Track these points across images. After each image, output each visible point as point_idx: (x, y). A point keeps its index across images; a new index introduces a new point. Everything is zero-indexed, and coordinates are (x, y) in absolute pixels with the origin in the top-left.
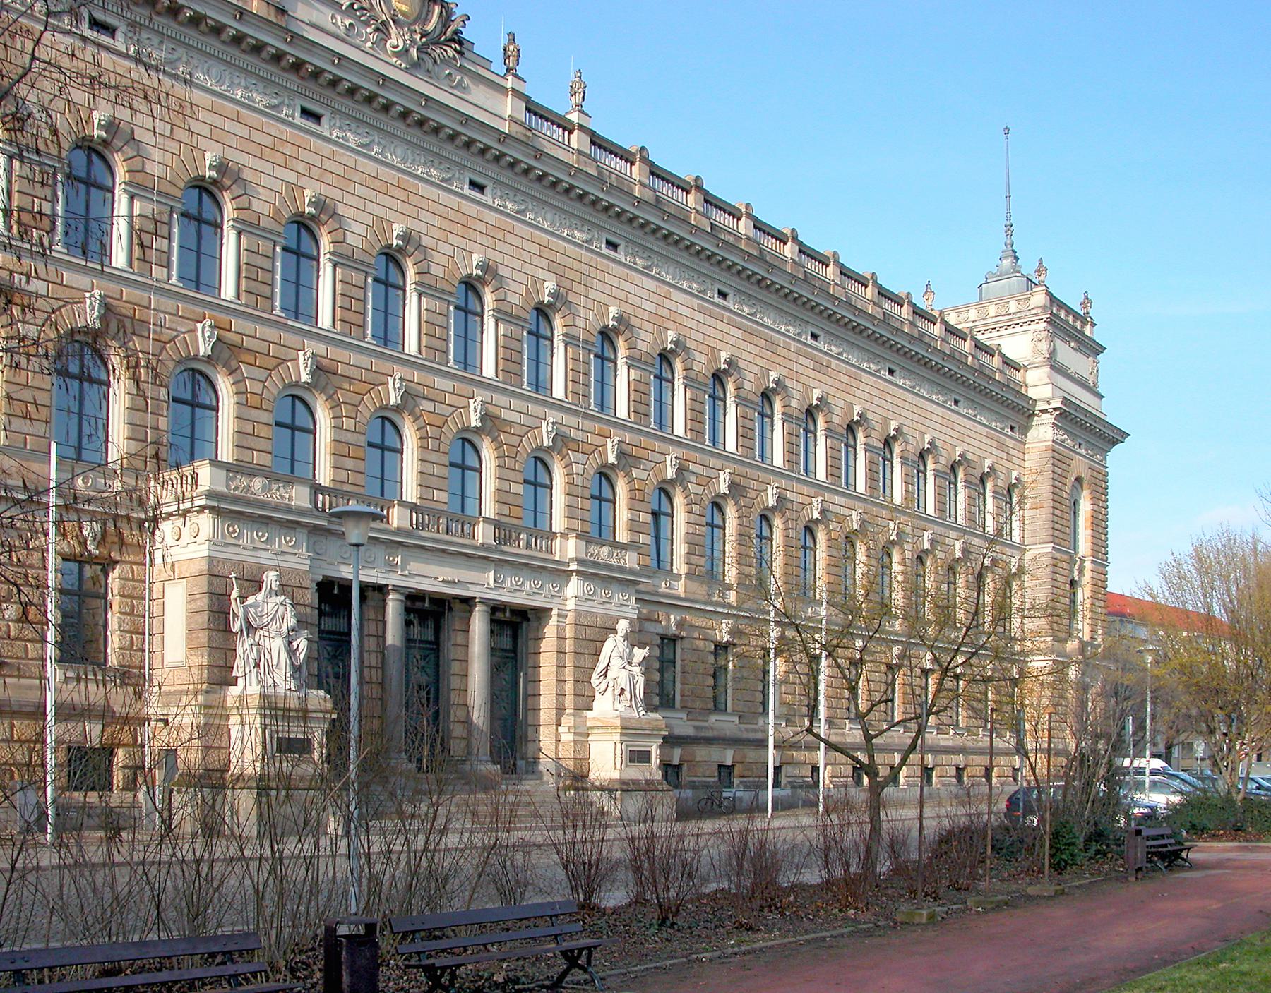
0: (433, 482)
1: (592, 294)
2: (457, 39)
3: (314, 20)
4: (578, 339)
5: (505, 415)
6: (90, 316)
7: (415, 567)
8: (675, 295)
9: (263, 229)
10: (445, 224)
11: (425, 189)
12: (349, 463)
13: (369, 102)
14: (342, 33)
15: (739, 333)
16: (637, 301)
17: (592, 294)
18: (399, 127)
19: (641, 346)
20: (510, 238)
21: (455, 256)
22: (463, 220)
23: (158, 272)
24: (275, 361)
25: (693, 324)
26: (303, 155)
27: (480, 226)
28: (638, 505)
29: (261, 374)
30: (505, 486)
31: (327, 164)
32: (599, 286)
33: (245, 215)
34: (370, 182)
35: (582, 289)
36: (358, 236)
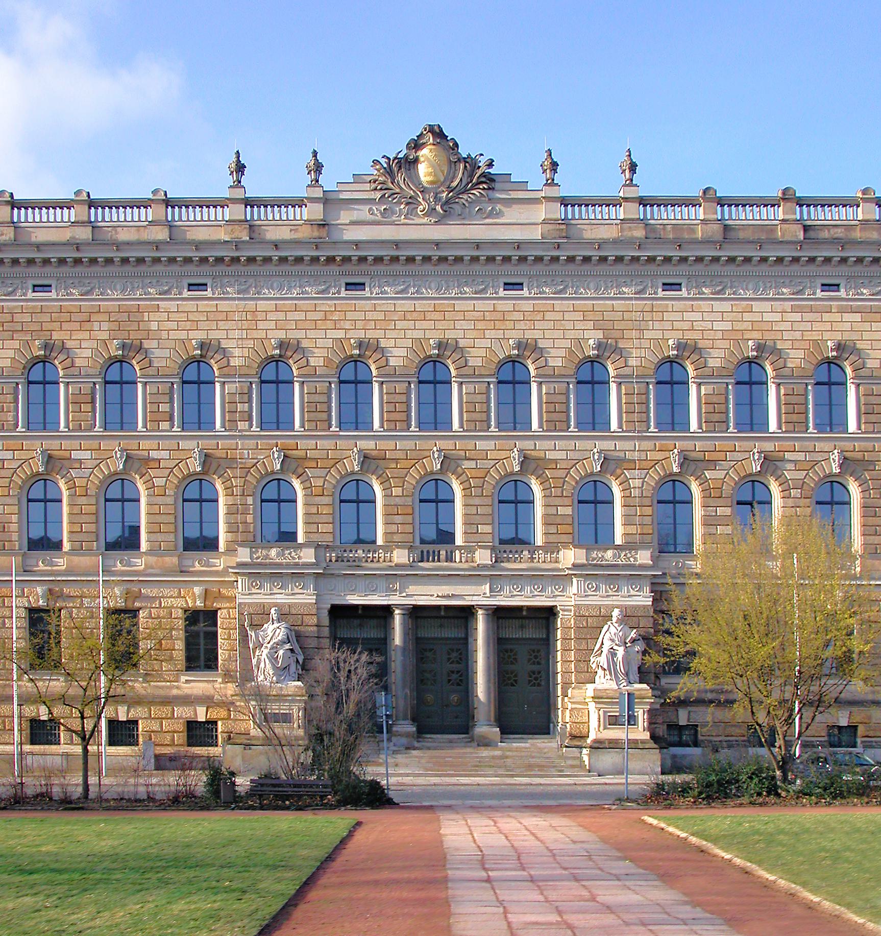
0: (477, 519)
1: (647, 335)
2: (489, 180)
3: (354, 218)
4: (631, 376)
5: (550, 455)
6: (195, 466)
7: (412, 589)
8: (757, 306)
9: (320, 376)
10: (480, 325)
11: (460, 305)
12: (398, 519)
14: (379, 218)
15: (857, 317)
17: (647, 335)
18: (428, 267)
19: (712, 363)
20: (548, 316)
21: (484, 348)
22: (499, 316)
23: (242, 425)
25: (788, 326)
26: (350, 315)
27: (518, 316)
28: (711, 502)
29: (323, 472)
30: (552, 511)
31: (370, 316)
32: (657, 325)
33: (304, 371)
34: (409, 316)
35: (634, 334)
36: (398, 357)
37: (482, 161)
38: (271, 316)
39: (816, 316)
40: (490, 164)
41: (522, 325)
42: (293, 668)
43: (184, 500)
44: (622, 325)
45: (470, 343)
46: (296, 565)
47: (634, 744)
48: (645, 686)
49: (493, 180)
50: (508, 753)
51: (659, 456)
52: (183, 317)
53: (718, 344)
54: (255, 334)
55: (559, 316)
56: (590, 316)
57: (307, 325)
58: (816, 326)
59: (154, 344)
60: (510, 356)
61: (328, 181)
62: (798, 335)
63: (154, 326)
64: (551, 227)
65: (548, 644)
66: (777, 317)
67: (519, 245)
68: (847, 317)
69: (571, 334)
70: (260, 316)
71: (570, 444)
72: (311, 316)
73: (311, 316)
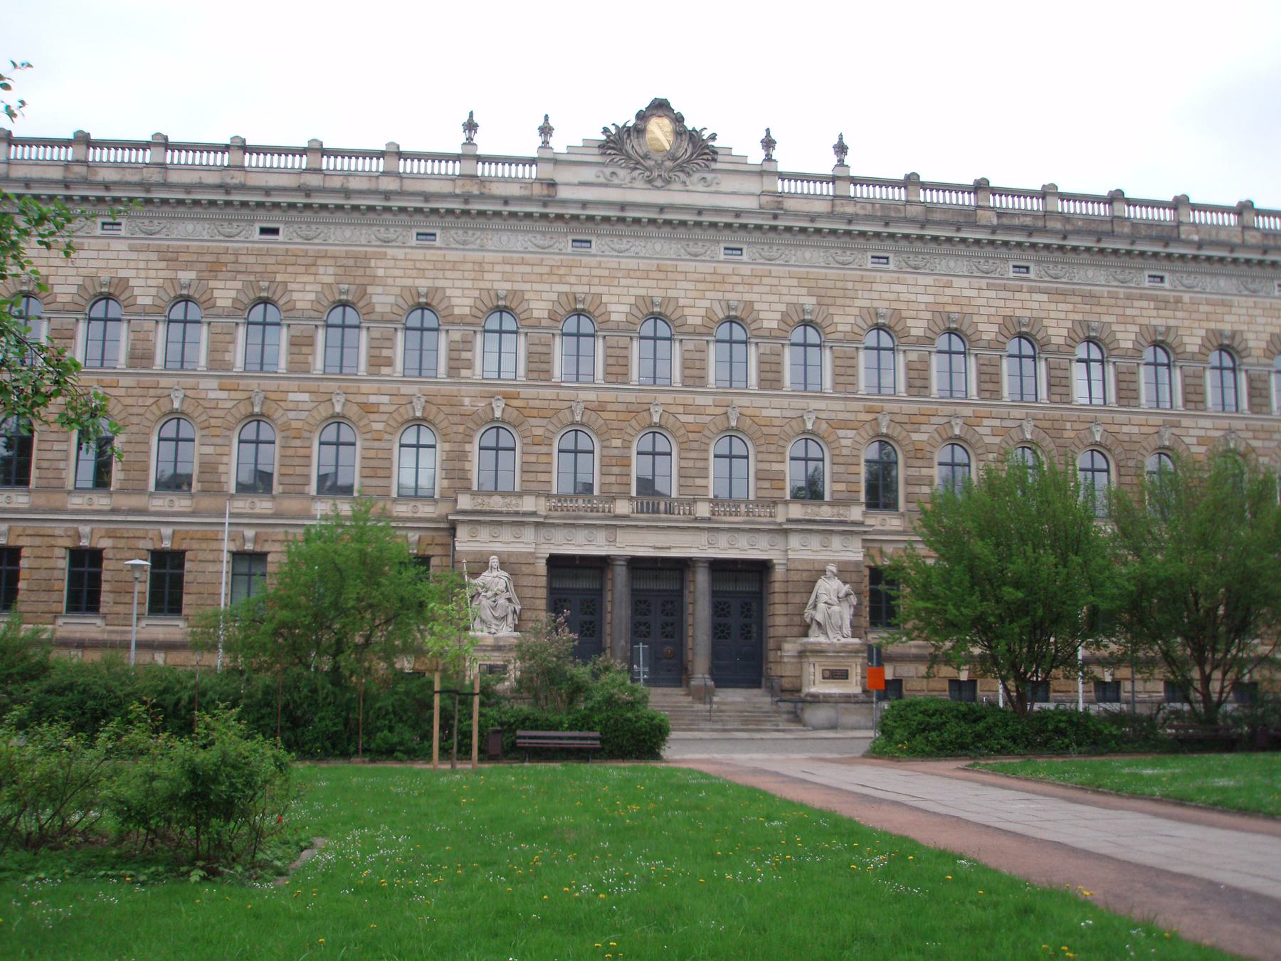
3: (582, 180)
9: (544, 328)
10: (701, 286)
13: (622, 221)
15: (1045, 297)
16: (913, 297)
20: (765, 281)
22: (719, 278)
24: (552, 412)
25: (984, 302)
27: (738, 279)
31: (595, 272)
32: (866, 295)
37: (706, 135)
38: (497, 268)
39: (1009, 295)
40: (713, 137)
41: (740, 288)
42: (510, 618)
43: (401, 446)
44: (835, 293)
45: (690, 302)
46: (517, 513)
47: (847, 699)
48: (857, 640)
49: (716, 153)
50: (723, 708)
51: (869, 417)
52: (410, 264)
53: (922, 315)
54: (482, 285)
55: (775, 281)
56: (805, 283)
57: (534, 278)
58: (1010, 304)
59: (380, 290)
60: (728, 317)
61: (559, 144)
62: (993, 311)
63: (380, 272)
64: (768, 198)
65: (761, 598)
66: (974, 293)
67: (738, 214)
68: (1036, 297)
69: (787, 299)
70: (488, 267)
71: (785, 402)
72: (538, 269)
73: (538, 269)
